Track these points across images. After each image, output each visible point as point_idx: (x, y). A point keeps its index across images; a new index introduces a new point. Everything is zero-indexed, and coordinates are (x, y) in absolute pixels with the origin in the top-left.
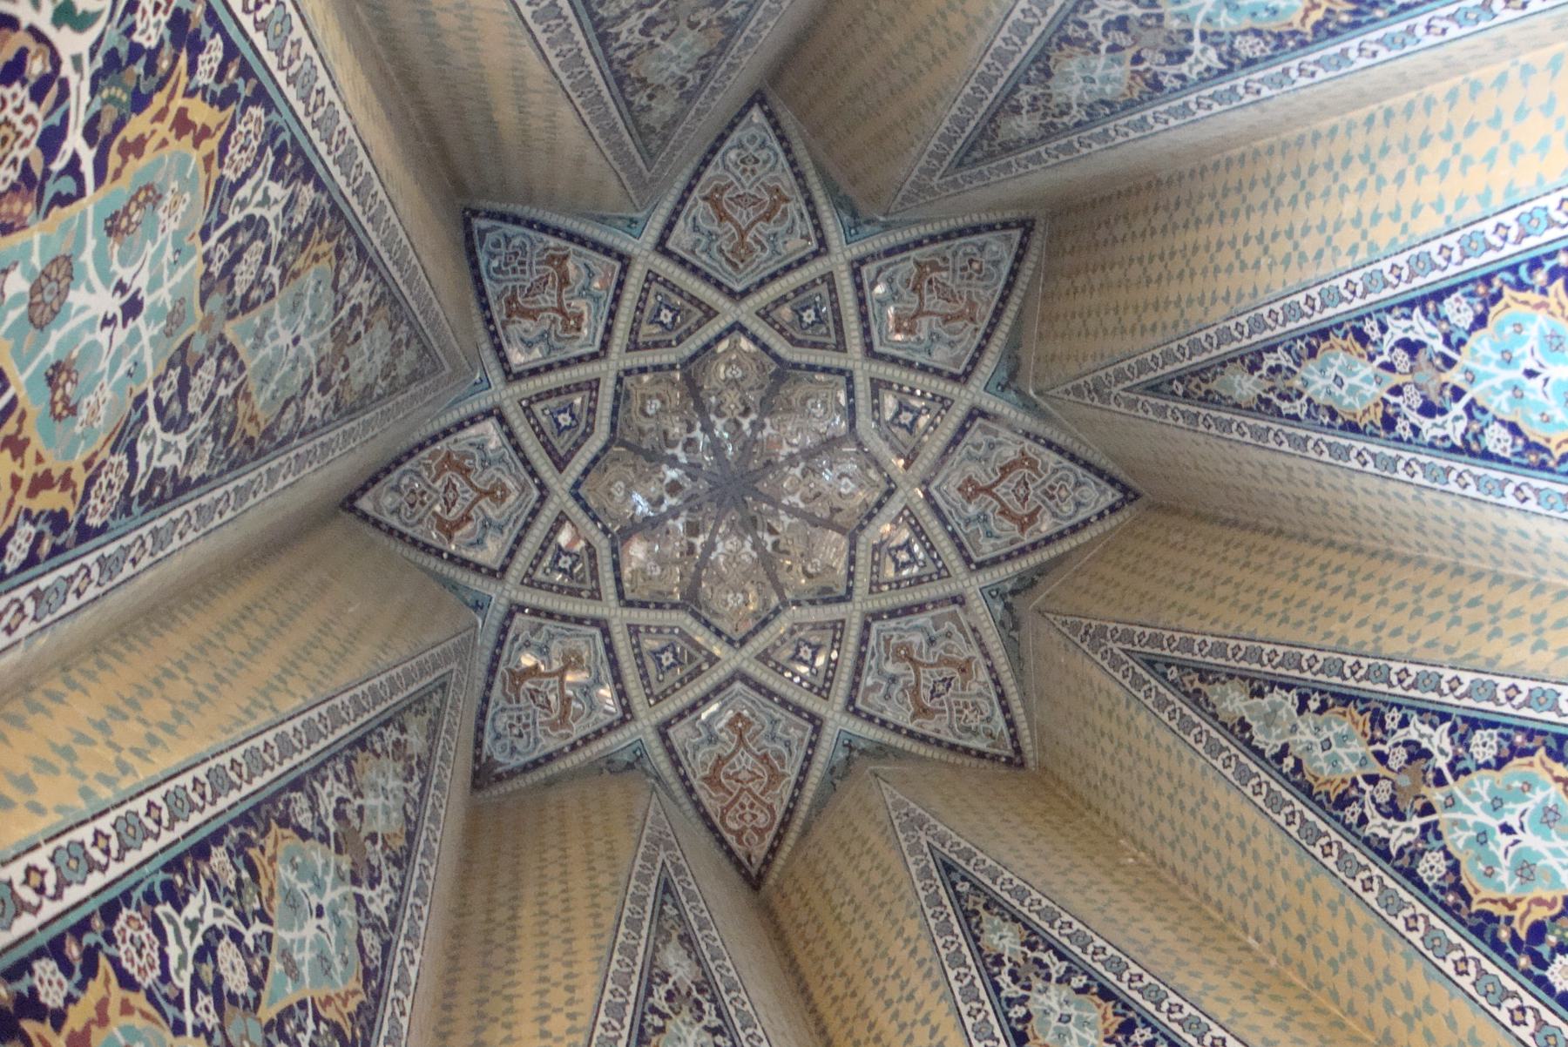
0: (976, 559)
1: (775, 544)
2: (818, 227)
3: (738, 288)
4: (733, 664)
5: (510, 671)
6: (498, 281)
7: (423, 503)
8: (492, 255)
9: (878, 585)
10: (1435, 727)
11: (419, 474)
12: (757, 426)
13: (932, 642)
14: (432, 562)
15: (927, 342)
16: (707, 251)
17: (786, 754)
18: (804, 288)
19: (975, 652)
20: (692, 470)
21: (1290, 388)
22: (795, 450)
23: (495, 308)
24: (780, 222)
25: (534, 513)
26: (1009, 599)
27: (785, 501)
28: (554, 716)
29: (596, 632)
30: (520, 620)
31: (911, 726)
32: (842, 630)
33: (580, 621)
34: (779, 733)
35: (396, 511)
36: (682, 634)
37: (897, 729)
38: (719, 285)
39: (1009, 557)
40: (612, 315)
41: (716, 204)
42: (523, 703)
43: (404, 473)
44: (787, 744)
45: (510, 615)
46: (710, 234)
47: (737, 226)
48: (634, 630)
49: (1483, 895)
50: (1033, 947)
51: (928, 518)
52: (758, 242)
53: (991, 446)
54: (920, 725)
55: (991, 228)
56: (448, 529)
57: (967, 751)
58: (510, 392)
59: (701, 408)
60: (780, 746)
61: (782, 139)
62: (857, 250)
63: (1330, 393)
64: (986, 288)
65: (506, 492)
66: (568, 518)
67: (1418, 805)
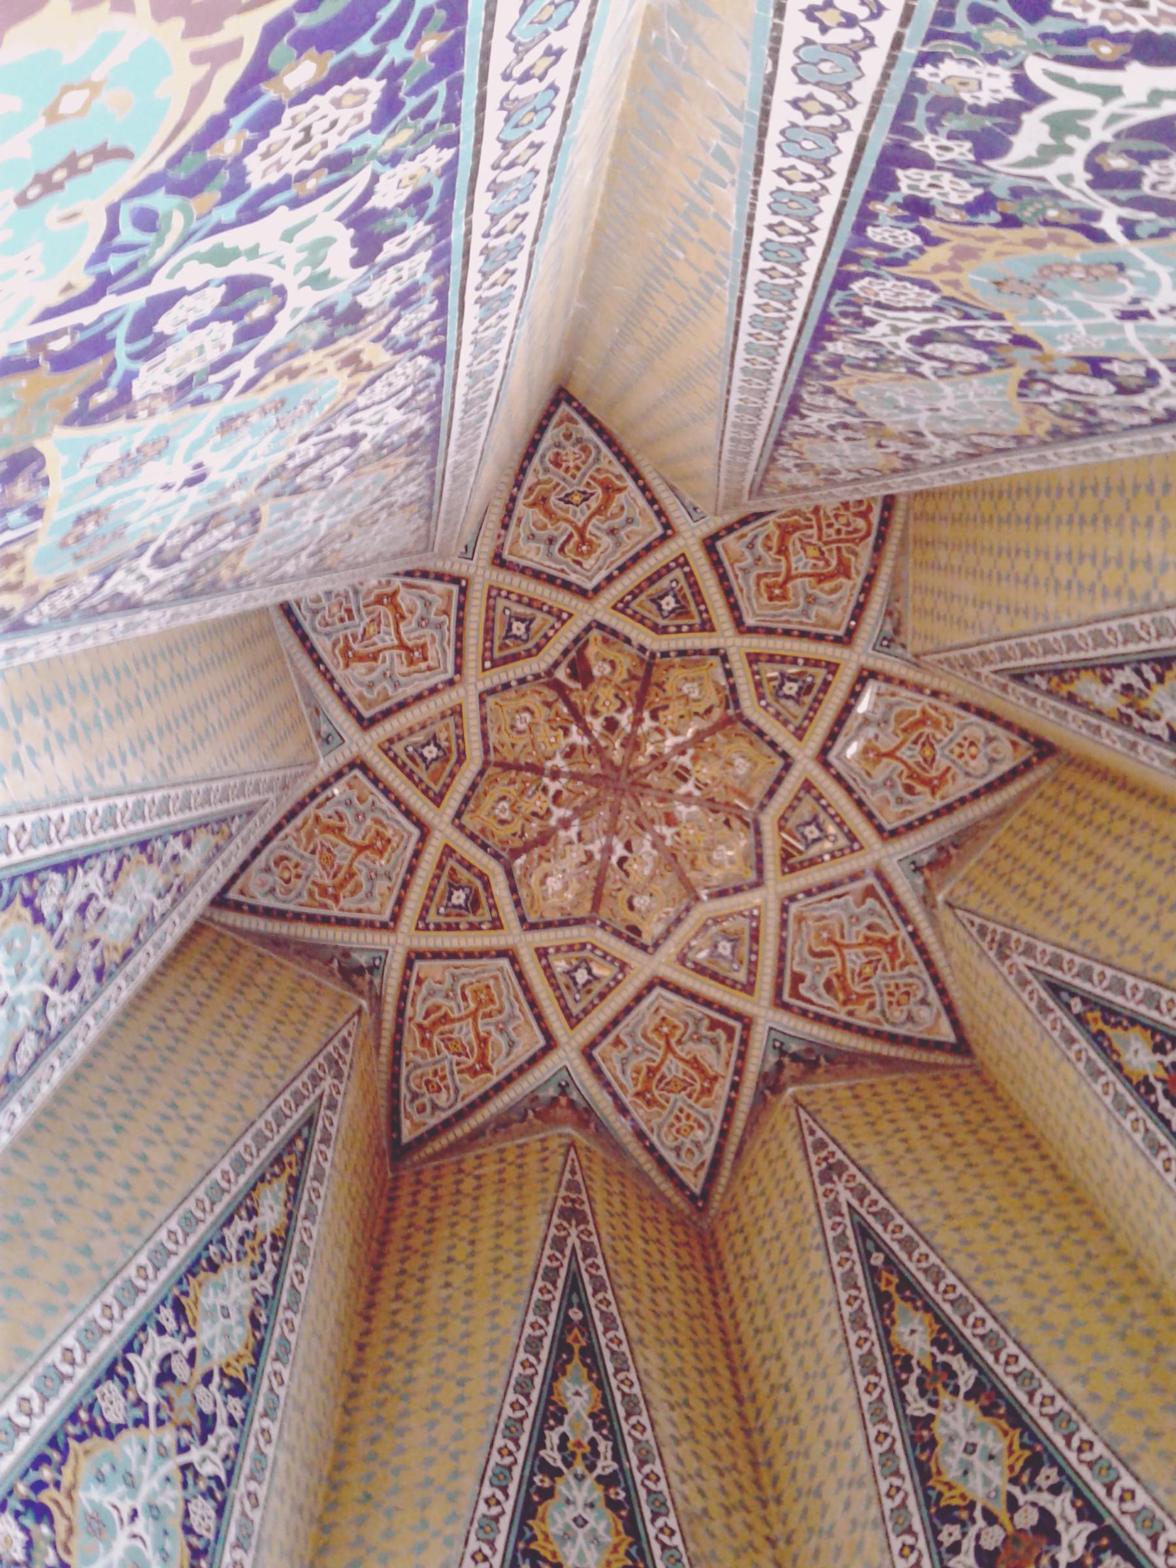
0: (455, 589)
1: (620, 710)
2: (405, 982)
3: (505, 963)
5: (933, 793)
6: (707, 1118)
8: (698, 1144)
9: (559, 618)
11: (883, 1013)
12: (565, 824)
13: (551, 541)
14: (928, 935)
17: (759, 542)
18: (450, 928)
19: (520, 508)
20: (646, 824)
22: (546, 781)
24: (438, 1008)
25: (808, 893)
27: (586, 741)
28: (927, 730)
29: (832, 757)
31: (630, 483)
33: (838, 778)
34: (750, 560)
35: (924, 1002)
36: (761, 697)
37: (645, 489)
38: (520, 975)
40: (627, 1010)
41: (482, 1058)
43: (894, 1024)
44: (751, 546)
48: (800, 733)
52: (465, 998)
53: (371, 686)
54: (619, 477)
55: (254, 910)
57: (601, 431)
59: (600, 879)
60: (760, 549)
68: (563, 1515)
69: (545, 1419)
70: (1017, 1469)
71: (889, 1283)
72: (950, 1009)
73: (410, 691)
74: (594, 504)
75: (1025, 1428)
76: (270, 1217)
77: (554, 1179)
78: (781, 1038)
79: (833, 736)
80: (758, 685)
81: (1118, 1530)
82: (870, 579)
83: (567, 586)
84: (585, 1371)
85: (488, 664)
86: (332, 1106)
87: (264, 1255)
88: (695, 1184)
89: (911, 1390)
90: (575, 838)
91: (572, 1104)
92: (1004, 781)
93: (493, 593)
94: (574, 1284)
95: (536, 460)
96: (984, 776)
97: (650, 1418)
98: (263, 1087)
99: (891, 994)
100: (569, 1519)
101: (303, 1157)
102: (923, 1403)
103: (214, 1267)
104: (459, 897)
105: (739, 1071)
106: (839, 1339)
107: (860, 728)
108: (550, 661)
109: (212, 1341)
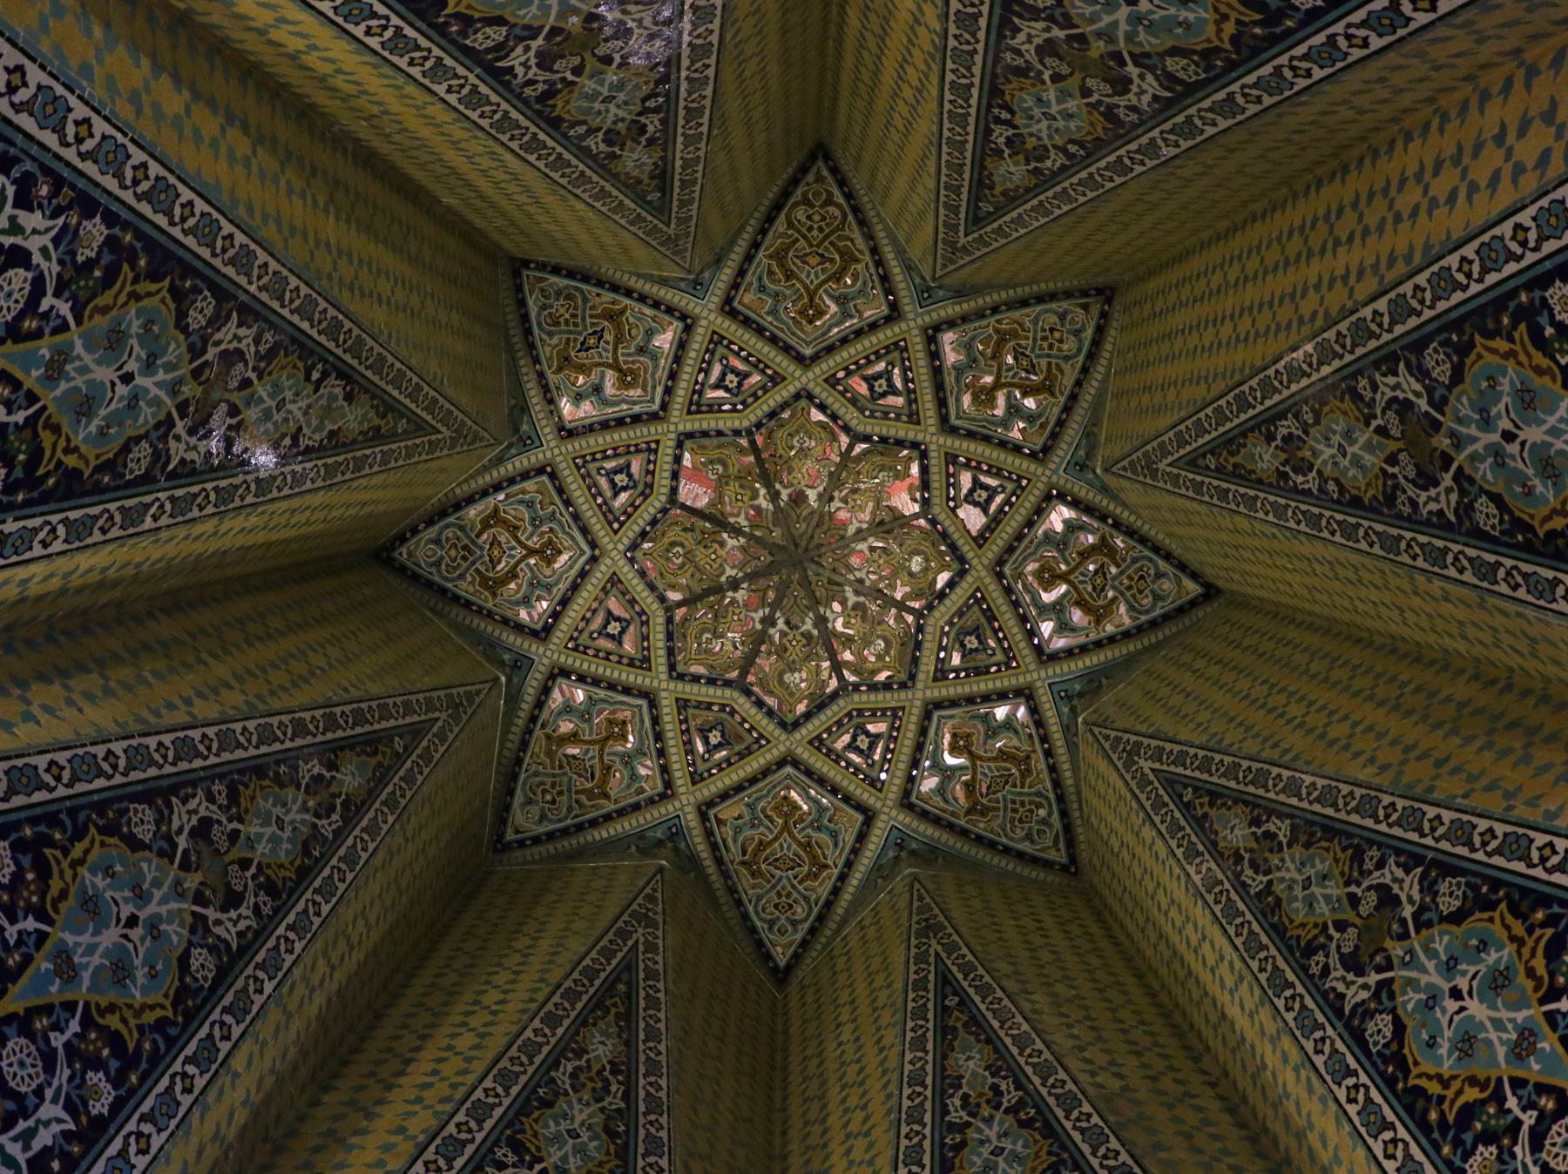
0: (544, 478)
1: (755, 495)
2: (709, 833)
3: (789, 769)
4: (810, 375)
5: (1053, 394)
6: (1039, 794)
7: (1130, 578)
8: (1044, 822)
9: (649, 450)
10: (183, 461)
13: (597, 389)
15: (594, 710)
16: (822, 810)
19: (552, 378)
20: (837, 578)
21: (316, 794)
23: (1042, 766)
25: (1010, 549)
26: (514, 439)
29: (954, 421)
30: (1038, 444)
31: (627, 301)
32: (691, 403)
33: (971, 435)
35: (1159, 575)
37: (642, 299)
39: (512, 481)
42: (1044, 362)
44: (762, 289)
45: (1046, 450)
46: (819, 829)
47: (790, 834)
48: (914, 418)
49: (155, 301)
50: (613, 156)
51: (594, 520)
56: (1104, 547)
57: (571, 275)
58: (1029, 678)
61: (753, 930)
62: (667, 809)
63: (285, 805)
64: (537, 774)
65: (1038, 575)
66: (974, 539)
67: (207, 372)
68: (979, 1155)
69: (943, 1092)
70: (1347, 870)
71: (1202, 805)
72: (1182, 567)
73: (563, 586)
74: (609, 337)
75: (1340, 833)
76: (601, 1048)
77: (905, 914)
78: (1063, 686)
79: (942, 403)
80: (854, 402)
81: (1441, 857)
82: (874, 251)
83: (636, 419)
84: (972, 1038)
85: (616, 526)
86: (651, 948)
87: (607, 1082)
88: (1060, 856)
89: (1249, 872)
90: (786, 628)
91: (913, 853)
92: (1097, 343)
93: (582, 463)
94: (945, 980)
95: (536, 330)
96: (1079, 350)
97: (1044, 1042)
98: (566, 959)
99: (1129, 588)
100: (985, 1155)
101: (630, 997)
102: (1260, 878)
103: (550, 1105)
104: (715, 738)
105: (1044, 739)
106: (1183, 879)
107: (958, 380)
108: (665, 490)
109: (565, 1159)
